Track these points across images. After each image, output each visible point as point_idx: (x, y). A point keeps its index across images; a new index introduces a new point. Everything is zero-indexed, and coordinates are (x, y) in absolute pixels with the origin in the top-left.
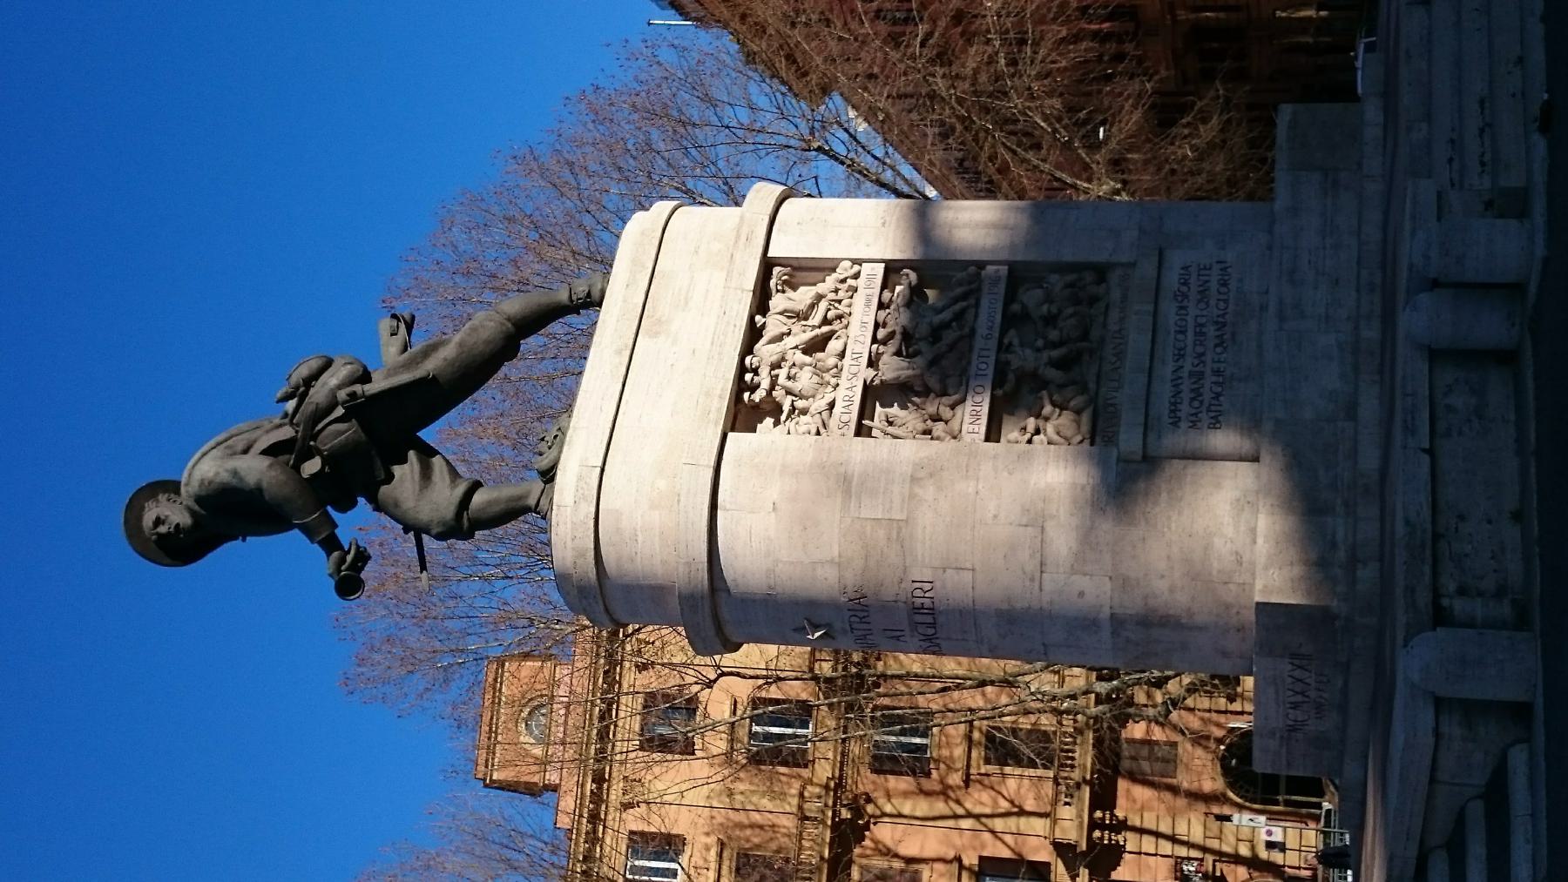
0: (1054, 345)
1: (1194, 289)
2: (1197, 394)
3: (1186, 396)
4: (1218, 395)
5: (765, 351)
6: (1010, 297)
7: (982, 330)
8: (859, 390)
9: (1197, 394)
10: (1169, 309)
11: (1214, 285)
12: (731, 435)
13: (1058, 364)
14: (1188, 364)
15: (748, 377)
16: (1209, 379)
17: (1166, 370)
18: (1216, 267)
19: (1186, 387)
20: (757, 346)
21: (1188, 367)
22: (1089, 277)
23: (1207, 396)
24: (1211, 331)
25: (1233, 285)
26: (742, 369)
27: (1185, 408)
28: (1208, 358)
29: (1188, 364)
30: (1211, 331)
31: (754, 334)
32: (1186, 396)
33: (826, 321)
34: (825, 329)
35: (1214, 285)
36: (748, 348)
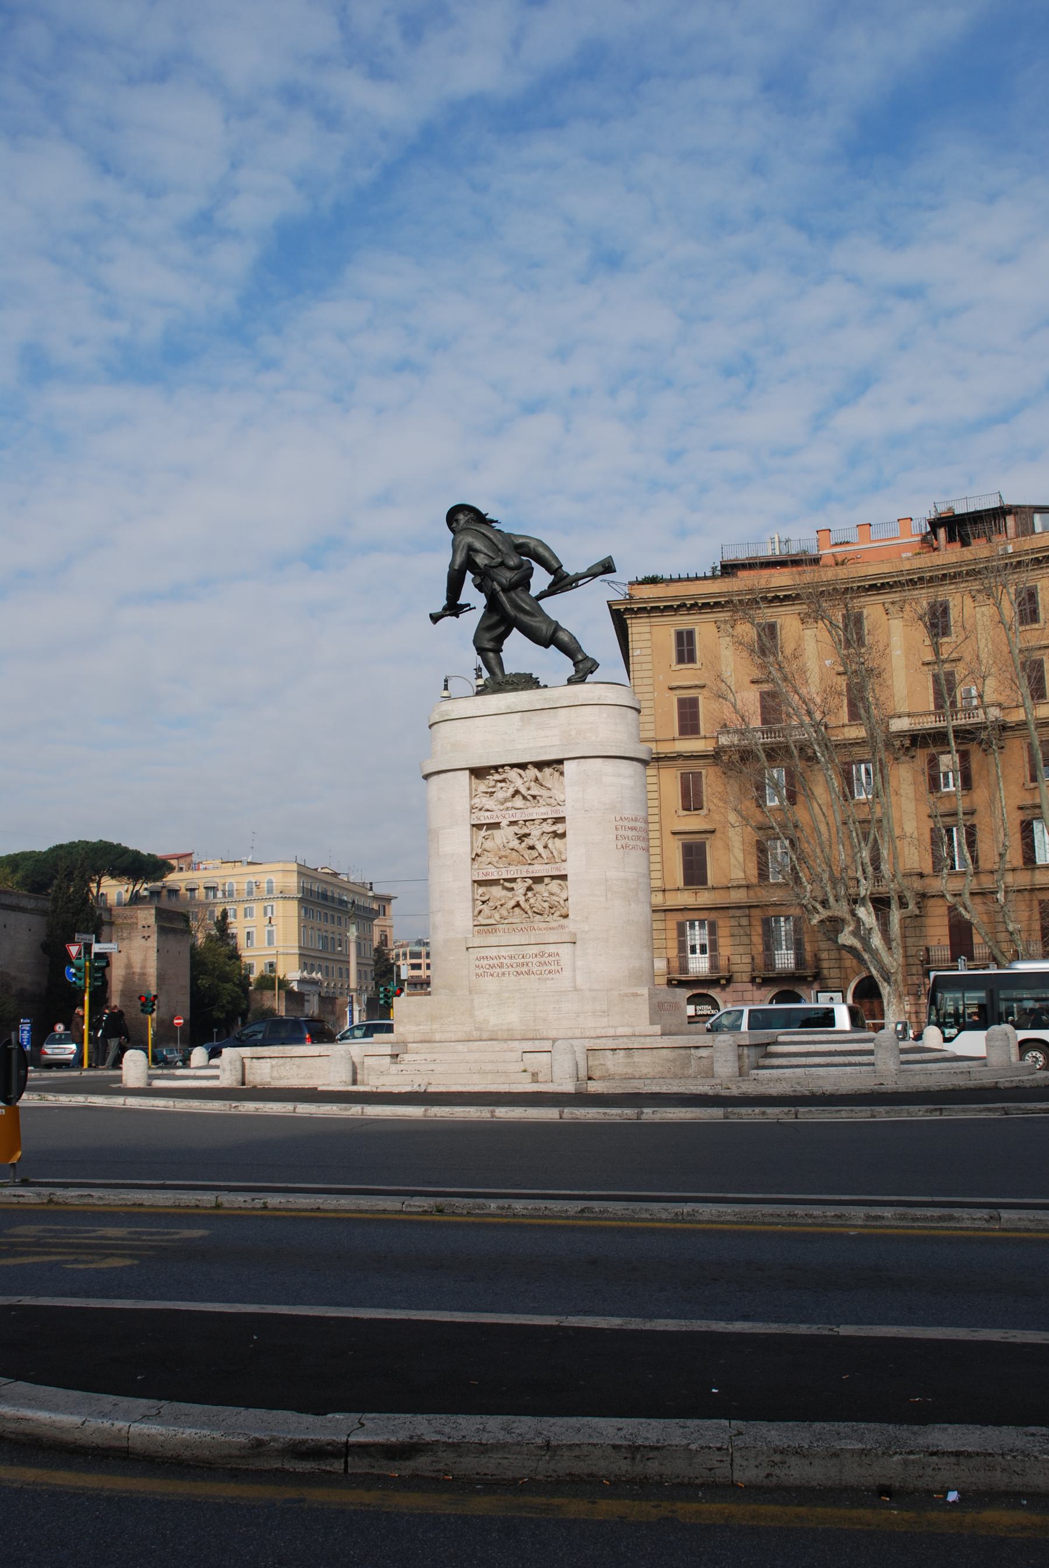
0: (527, 900)
1: (547, 960)
2: (492, 967)
3: (491, 962)
4: (492, 975)
5: (513, 774)
6: (553, 877)
7: (531, 868)
8: (497, 821)
9: (492, 967)
10: (535, 950)
11: (549, 968)
12: (467, 772)
13: (518, 905)
14: (508, 961)
15: (500, 770)
16: (498, 970)
17: (503, 951)
18: (559, 968)
19: (495, 962)
20: (515, 769)
21: (505, 961)
22: (564, 912)
23: (491, 971)
24: (525, 969)
25: (550, 976)
26: (503, 766)
27: (484, 962)
28: (510, 969)
29: (508, 961)
30: (525, 969)
31: (523, 766)
32: (491, 962)
33: (534, 797)
34: (529, 797)
35: (549, 968)
36: (512, 766)
